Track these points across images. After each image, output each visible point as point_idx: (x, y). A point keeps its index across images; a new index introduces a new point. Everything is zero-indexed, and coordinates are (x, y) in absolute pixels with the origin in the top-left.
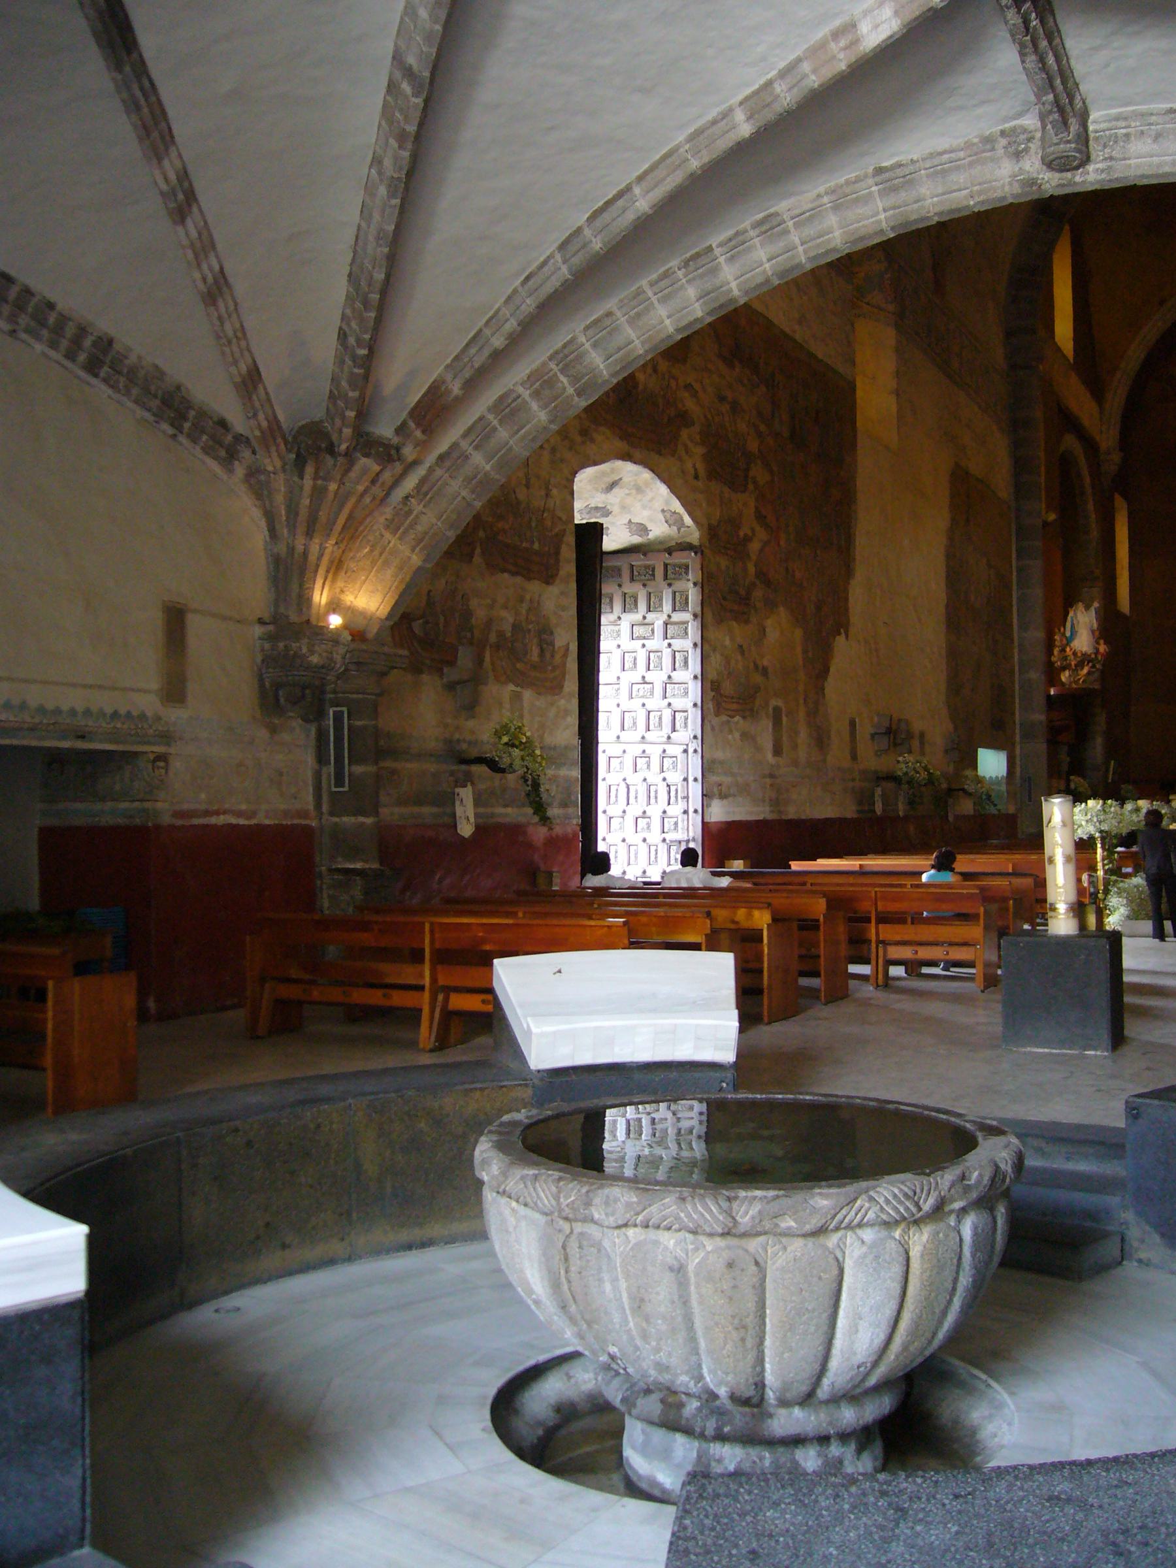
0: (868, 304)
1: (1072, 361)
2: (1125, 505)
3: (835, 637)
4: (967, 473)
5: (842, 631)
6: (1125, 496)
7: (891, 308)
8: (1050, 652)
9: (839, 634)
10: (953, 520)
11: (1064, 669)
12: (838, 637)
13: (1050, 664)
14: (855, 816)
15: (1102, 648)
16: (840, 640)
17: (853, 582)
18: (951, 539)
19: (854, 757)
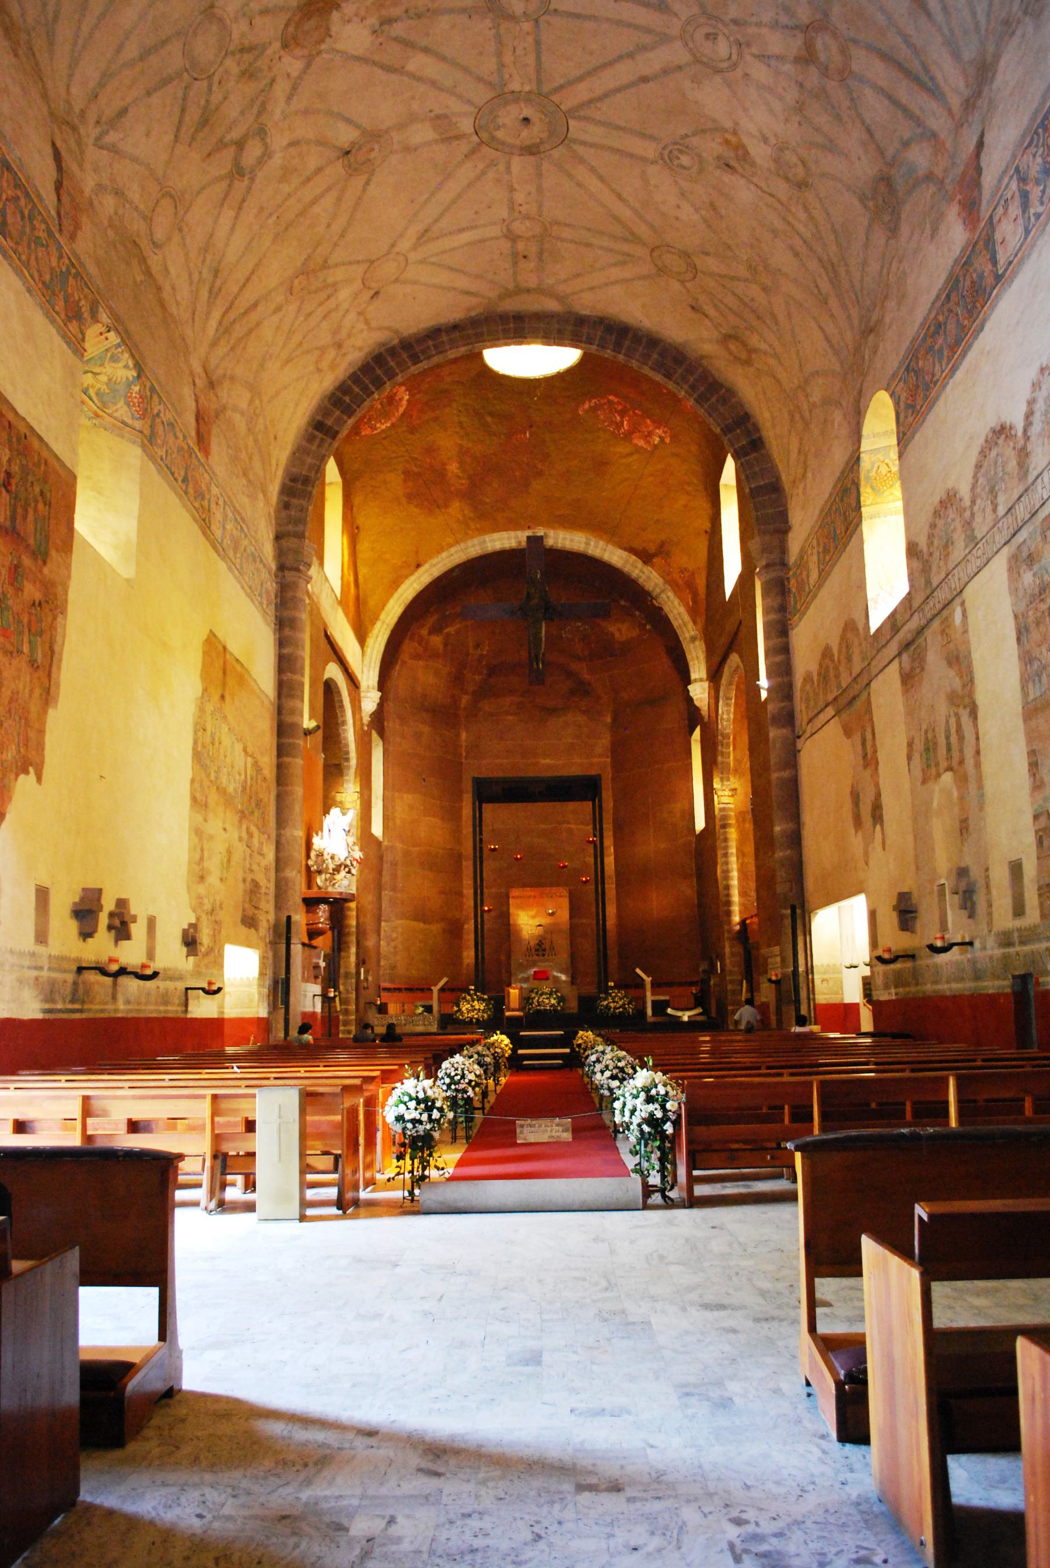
0: (110, 415)
1: (339, 595)
2: (381, 743)
3: (17, 776)
4: (225, 648)
5: (31, 769)
6: (382, 734)
7: (138, 424)
8: (308, 857)
9: (27, 772)
10: (205, 690)
11: (320, 872)
12: (22, 777)
13: (308, 868)
14: (40, 1016)
15: (358, 854)
16: (25, 783)
17: (51, 711)
18: (201, 710)
19: (41, 937)
